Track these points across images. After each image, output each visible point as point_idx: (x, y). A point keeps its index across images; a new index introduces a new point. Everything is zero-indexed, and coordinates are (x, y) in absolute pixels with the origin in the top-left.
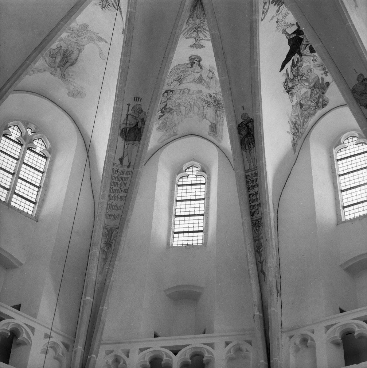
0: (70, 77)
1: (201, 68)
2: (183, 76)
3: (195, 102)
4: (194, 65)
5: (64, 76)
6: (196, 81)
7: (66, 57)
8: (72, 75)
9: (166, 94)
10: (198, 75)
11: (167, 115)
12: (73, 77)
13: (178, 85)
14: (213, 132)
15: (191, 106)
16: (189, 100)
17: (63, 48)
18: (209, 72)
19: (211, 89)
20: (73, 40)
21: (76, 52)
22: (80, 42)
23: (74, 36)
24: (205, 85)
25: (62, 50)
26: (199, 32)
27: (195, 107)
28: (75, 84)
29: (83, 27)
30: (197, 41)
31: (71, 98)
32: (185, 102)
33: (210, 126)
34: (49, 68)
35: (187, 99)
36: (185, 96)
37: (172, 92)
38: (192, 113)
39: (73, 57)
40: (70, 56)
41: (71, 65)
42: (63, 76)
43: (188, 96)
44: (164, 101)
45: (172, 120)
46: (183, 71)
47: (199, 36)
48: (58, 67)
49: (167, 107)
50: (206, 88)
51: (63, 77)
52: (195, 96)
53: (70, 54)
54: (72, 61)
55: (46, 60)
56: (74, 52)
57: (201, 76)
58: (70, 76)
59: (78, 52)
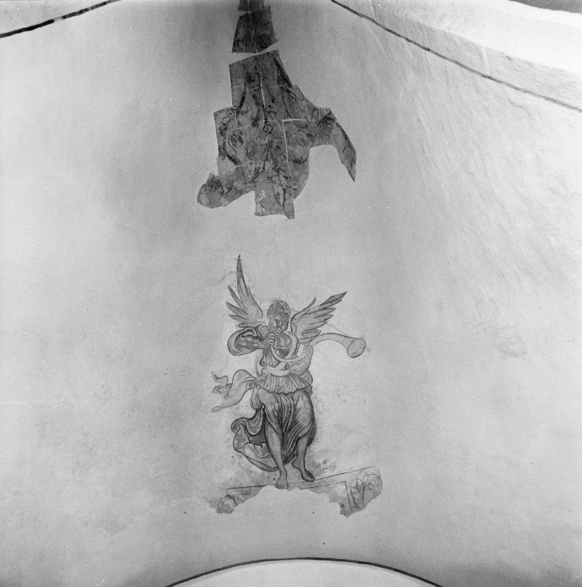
0: (324, 469)
5: (310, 475)
7: (290, 430)
8: (325, 462)
12: (328, 464)
17: (270, 409)
20: (279, 371)
21: (301, 403)
22: (296, 367)
23: (274, 360)
25: (272, 416)
28: (342, 478)
29: (278, 318)
31: (356, 515)
34: (266, 473)
39: (303, 417)
40: (295, 422)
41: (310, 442)
42: (309, 477)
48: (286, 461)
51: (309, 478)
53: (292, 415)
54: (306, 431)
55: (247, 457)
56: (298, 406)
58: (323, 466)
59: (305, 398)
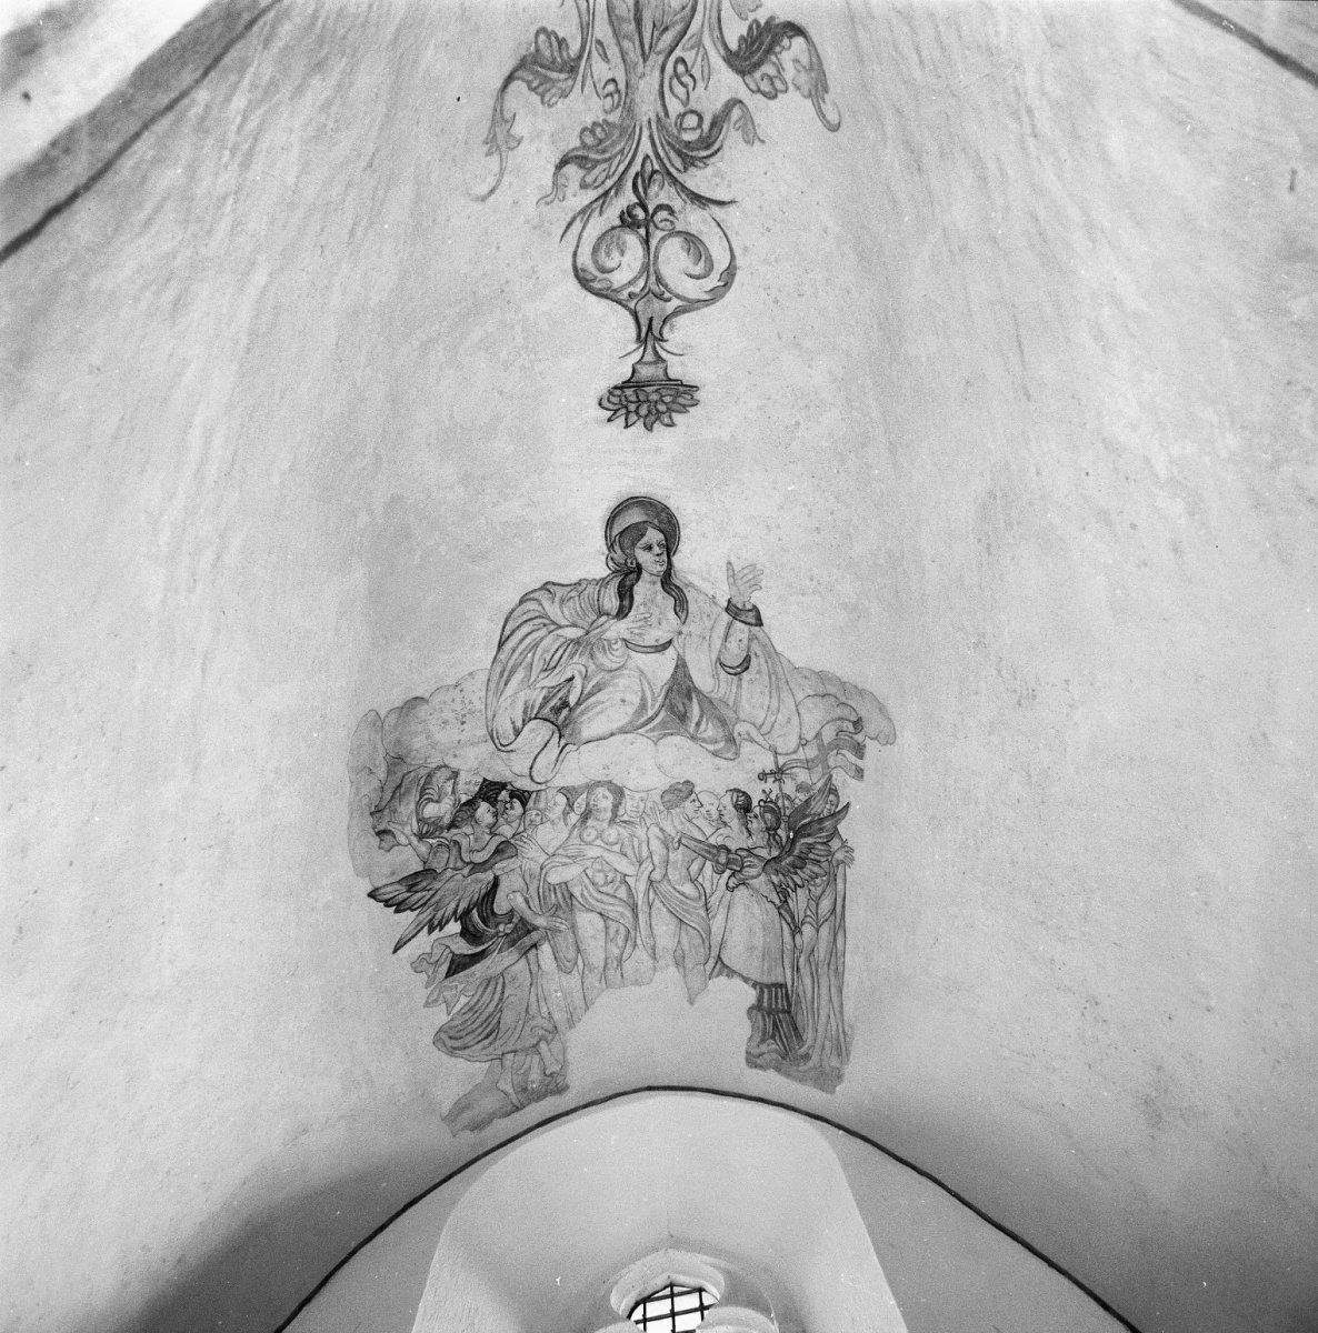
1: (681, 605)
2: (578, 681)
3: (657, 876)
4: (642, 590)
6: (652, 719)
9: (483, 809)
10: (662, 667)
11: (501, 960)
13: (553, 750)
14: (773, 1037)
15: (634, 908)
16: (624, 866)
18: (726, 618)
19: (747, 748)
24: (710, 730)
26: (659, 234)
27: (660, 911)
30: (649, 334)
32: (600, 879)
33: (758, 1007)
35: (610, 857)
36: (600, 836)
37: (524, 804)
38: (642, 954)
43: (612, 833)
44: (479, 858)
45: (533, 998)
46: (577, 642)
47: (659, 280)
49: (501, 905)
50: (715, 754)
52: (655, 830)
57: (681, 665)
